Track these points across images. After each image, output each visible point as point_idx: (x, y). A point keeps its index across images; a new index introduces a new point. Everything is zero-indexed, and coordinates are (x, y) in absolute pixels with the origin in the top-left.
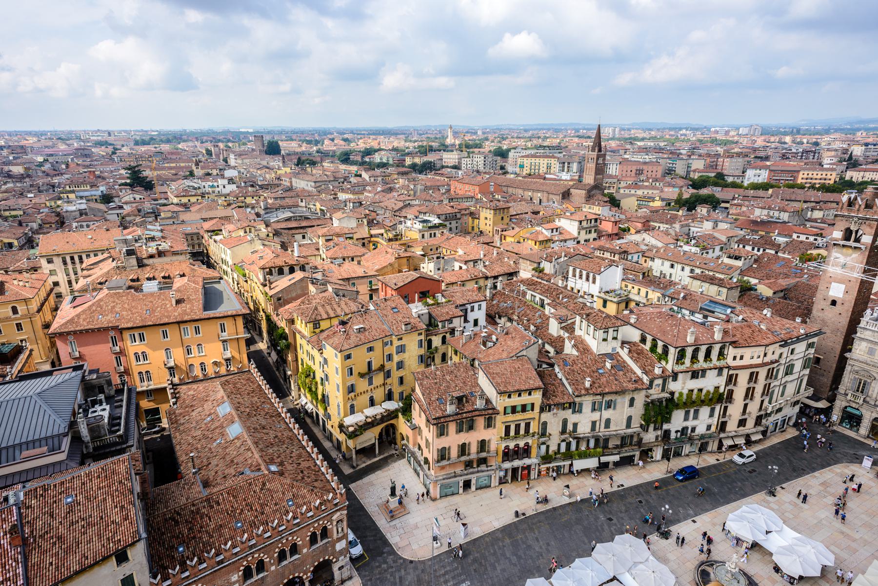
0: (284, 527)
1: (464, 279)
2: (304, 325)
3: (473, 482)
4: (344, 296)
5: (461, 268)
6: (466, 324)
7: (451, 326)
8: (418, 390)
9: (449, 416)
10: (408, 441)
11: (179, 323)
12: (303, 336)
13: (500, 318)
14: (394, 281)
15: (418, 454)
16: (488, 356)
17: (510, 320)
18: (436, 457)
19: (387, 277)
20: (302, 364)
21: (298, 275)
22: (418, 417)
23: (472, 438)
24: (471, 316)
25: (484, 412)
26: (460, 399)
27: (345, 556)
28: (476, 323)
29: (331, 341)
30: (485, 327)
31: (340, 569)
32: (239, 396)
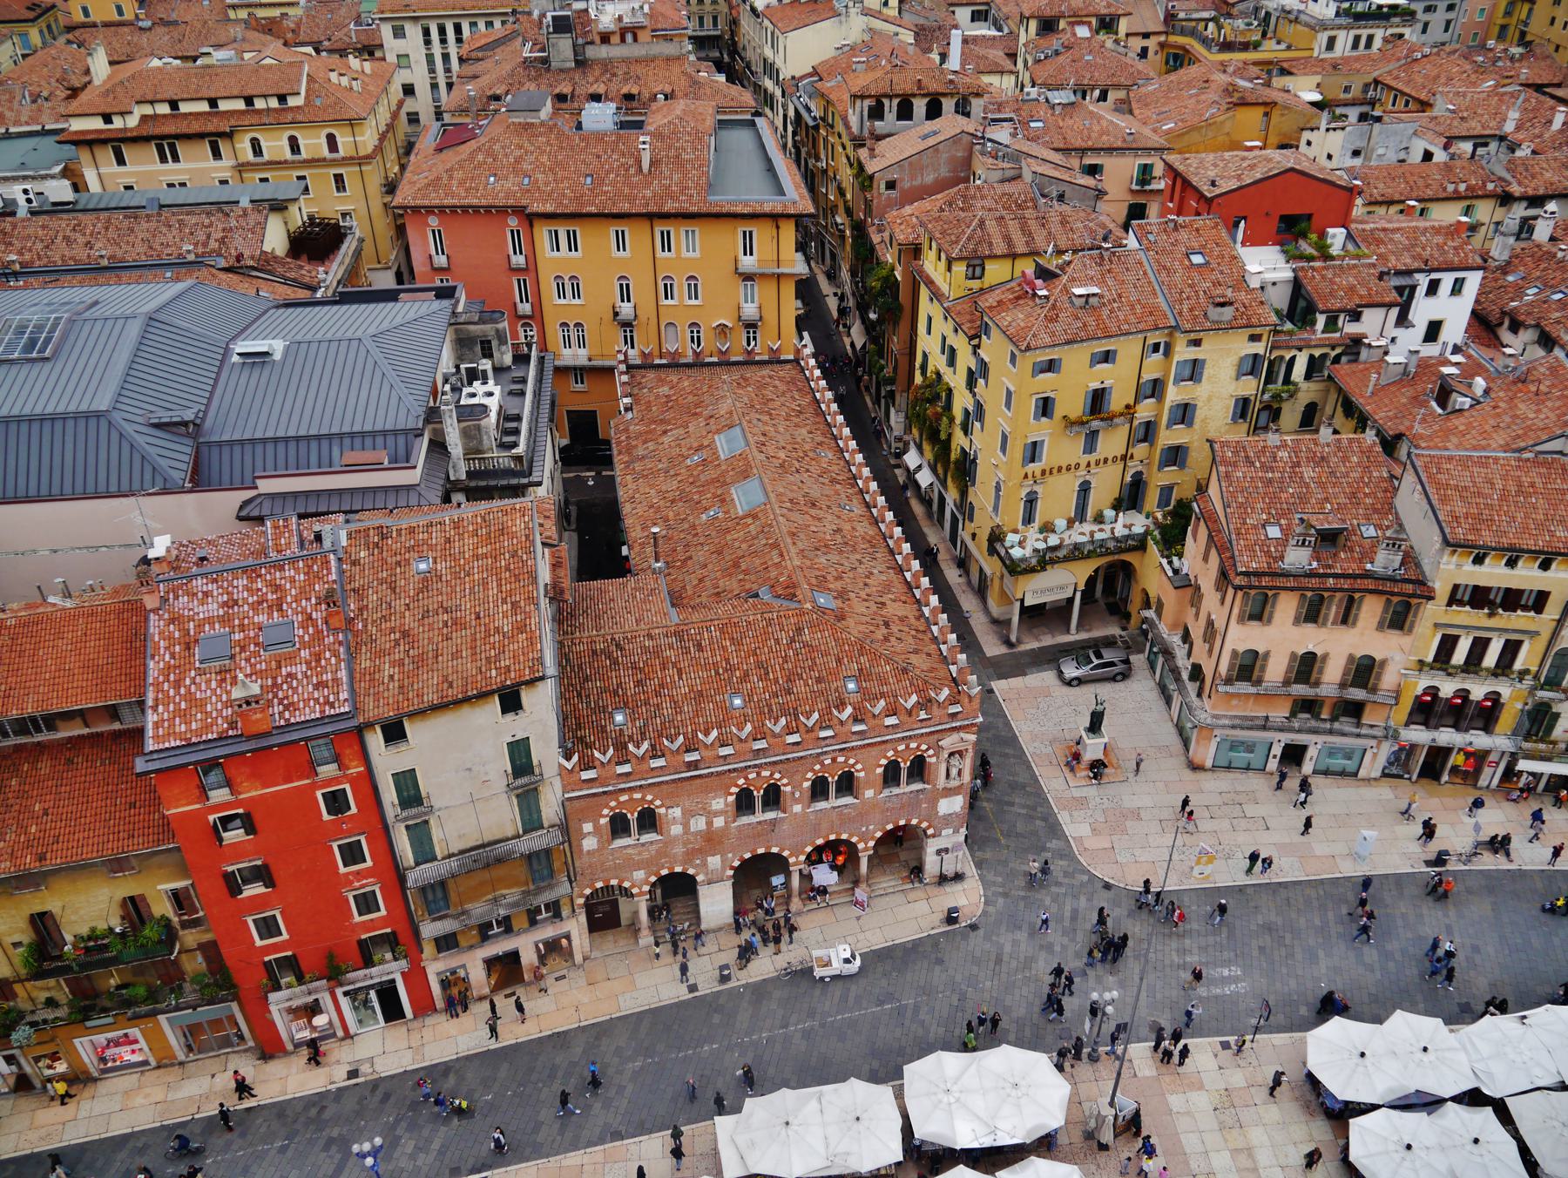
0: (829, 733)
1: (1429, 193)
2: (943, 264)
3: (1312, 752)
4: (1061, 198)
5: (1428, 156)
6: (1400, 333)
7: (1352, 329)
8: (1213, 490)
9: (1286, 575)
10: (1159, 613)
11: (652, 217)
12: (936, 295)
13: (1515, 327)
14: (1211, 174)
15: (1180, 652)
16: (1447, 433)
17: (1547, 341)
18: (1223, 669)
19: (1193, 160)
20: (924, 368)
21: (950, 123)
22: (1195, 558)
23: (1338, 645)
24: (1423, 310)
25: (1388, 586)
26: (1329, 538)
27: (956, 831)
28: (1433, 331)
29: (1006, 318)
30: (1457, 350)
31: (939, 852)
32: (766, 418)
